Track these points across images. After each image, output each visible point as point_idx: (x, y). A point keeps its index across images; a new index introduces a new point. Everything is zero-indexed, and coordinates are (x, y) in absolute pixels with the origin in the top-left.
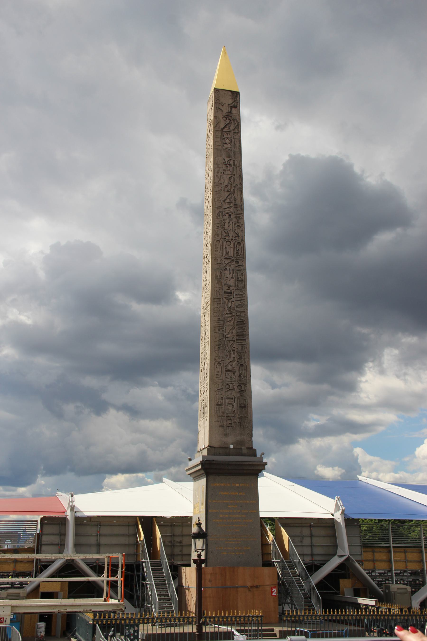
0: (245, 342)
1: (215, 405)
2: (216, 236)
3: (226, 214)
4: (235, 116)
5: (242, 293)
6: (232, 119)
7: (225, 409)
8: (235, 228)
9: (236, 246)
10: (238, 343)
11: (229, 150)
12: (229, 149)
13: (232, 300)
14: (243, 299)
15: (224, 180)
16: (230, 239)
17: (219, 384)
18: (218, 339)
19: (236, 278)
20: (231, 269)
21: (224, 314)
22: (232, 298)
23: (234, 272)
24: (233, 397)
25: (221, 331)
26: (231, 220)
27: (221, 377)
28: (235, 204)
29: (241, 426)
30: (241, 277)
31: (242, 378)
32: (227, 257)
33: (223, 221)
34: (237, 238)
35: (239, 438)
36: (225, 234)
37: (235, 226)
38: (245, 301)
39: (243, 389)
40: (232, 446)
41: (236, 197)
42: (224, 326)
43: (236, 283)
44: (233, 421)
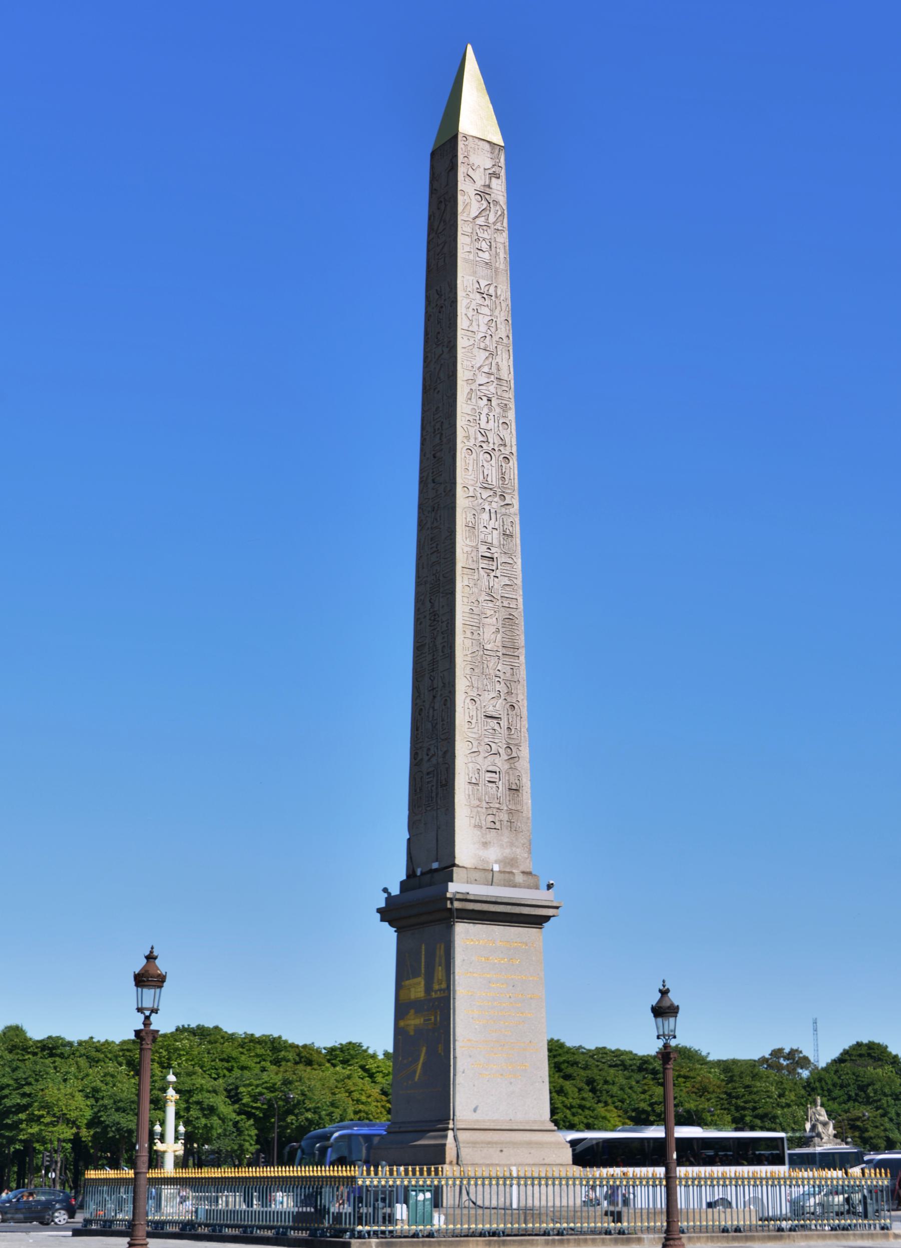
0: (517, 661)
1: (467, 783)
2: (465, 441)
3: (482, 397)
4: (497, 194)
5: (511, 562)
6: (490, 201)
7: (484, 793)
8: (498, 426)
9: (500, 464)
10: (505, 663)
11: (487, 263)
12: (487, 261)
13: (493, 574)
14: (513, 573)
15: (479, 326)
16: (490, 449)
17: (473, 742)
18: (470, 652)
19: (501, 531)
20: (493, 511)
21: (480, 601)
22: (493, 570)
23: (498, 516)
24: (498, 770)
25: (476, 636)
26: (492, 409)
27: (476, 728)
28: (498, 377)
29: (511, 827)
30: (511, 529)
31: (513, 732)
32: (484, 485)
33: (478, 411)
34: (502, 448)
35: (507, 851)
36: (481, 438)
37: (498, 422)
38: (516, 578)
39: (514, 755)
40: (496, 868)
41: (499, 364)
42: (481, 624)
43: (502, 540)
44: (497, 818)
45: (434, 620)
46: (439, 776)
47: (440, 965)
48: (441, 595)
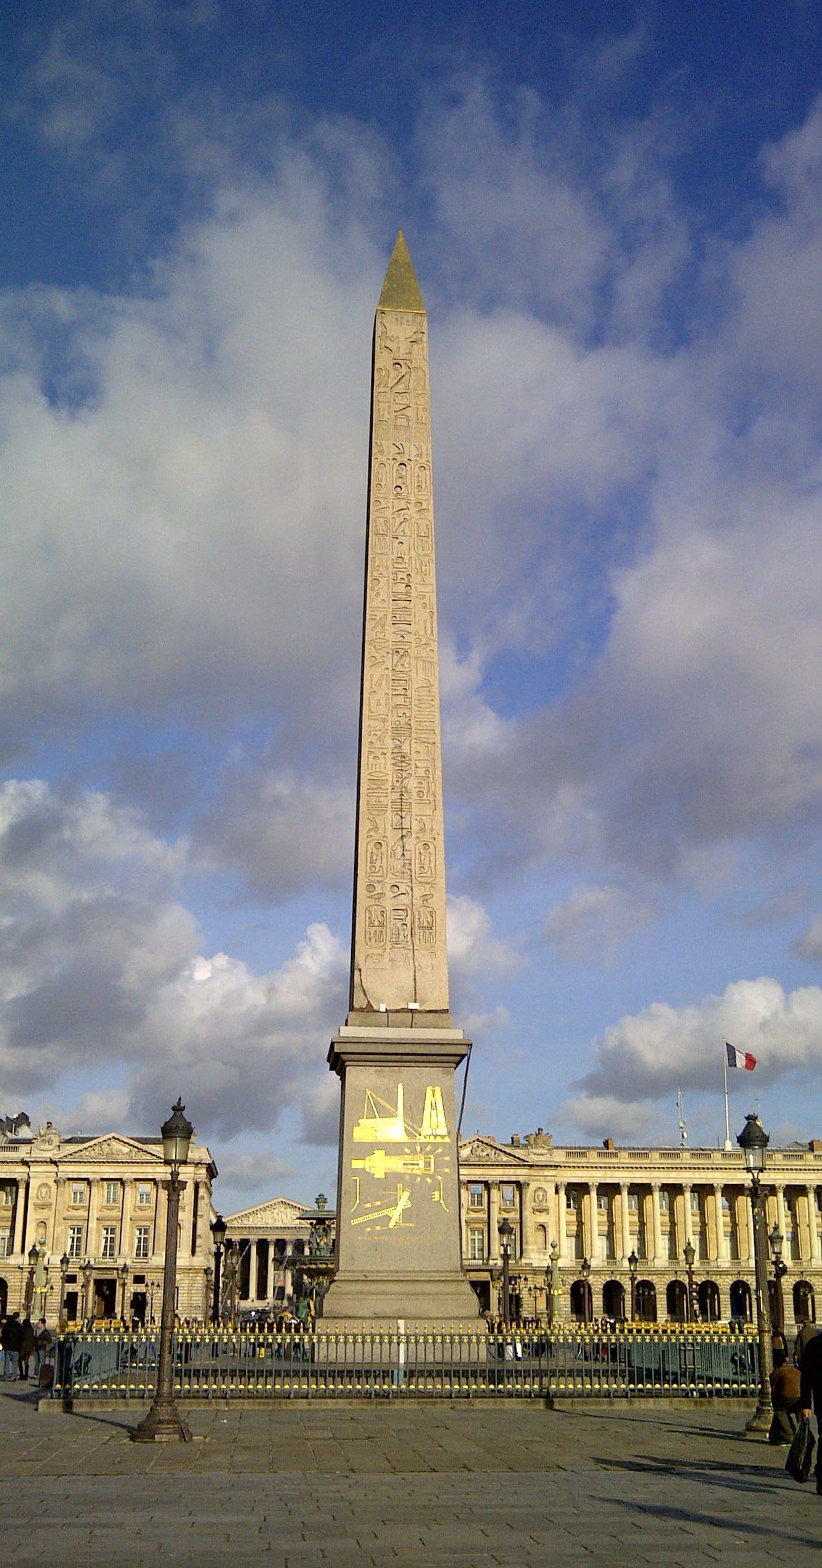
45: (402, 762)
46: (417, 917)
48: (414, 741)
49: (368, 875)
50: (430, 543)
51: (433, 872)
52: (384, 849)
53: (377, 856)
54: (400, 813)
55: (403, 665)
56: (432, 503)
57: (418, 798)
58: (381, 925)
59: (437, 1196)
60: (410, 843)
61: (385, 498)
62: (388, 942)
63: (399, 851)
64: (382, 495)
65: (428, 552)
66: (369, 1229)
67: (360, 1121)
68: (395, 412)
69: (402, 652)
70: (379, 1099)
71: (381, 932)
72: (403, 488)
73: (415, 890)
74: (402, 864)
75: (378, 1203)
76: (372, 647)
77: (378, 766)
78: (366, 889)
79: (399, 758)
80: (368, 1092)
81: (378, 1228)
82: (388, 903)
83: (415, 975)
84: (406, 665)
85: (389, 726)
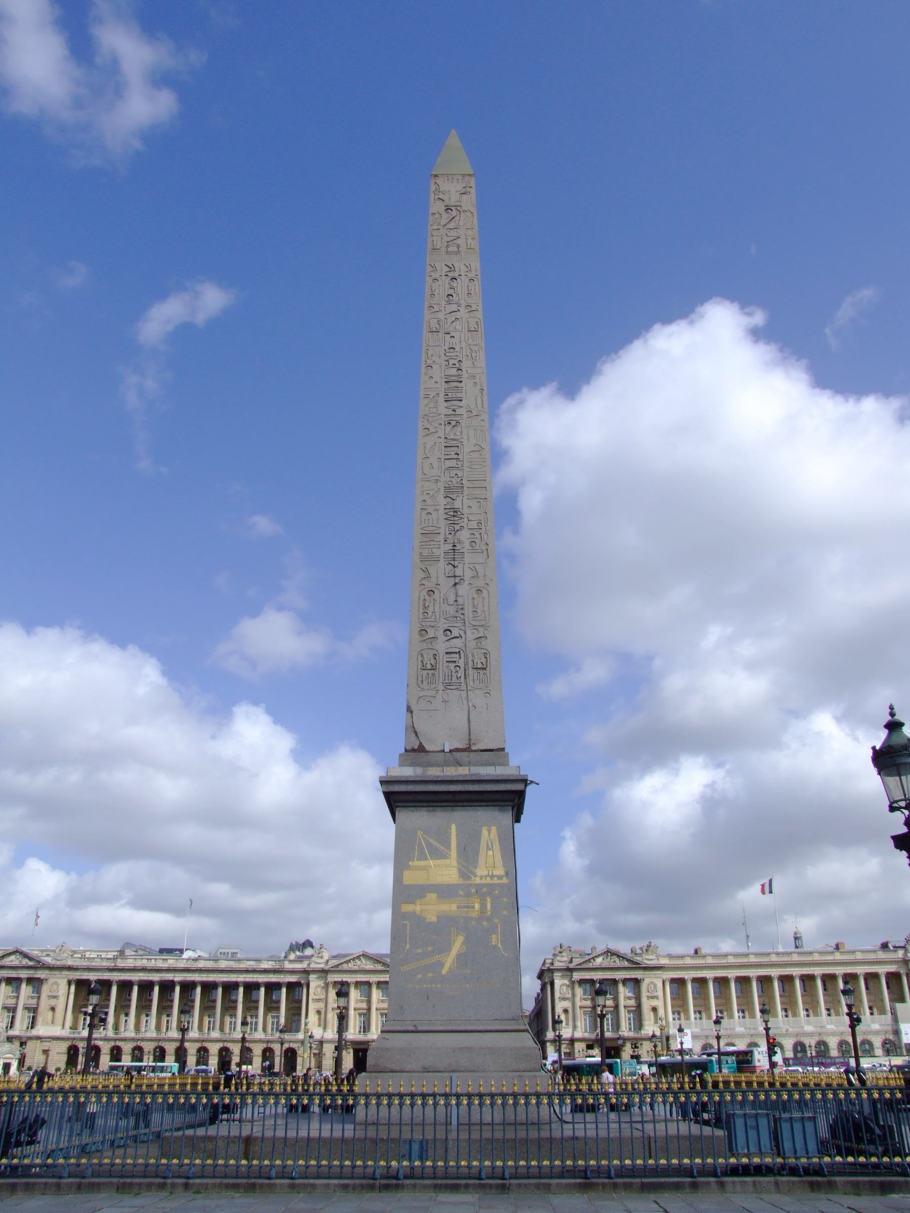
46: (470, 659)
47: (488, 849)
49: (420, 620)
50: (480, 336)
51: (487, 615)
52: (436, 596)
53: (430, 602)
54: (452, 562)
55: (455, 434)
56: (481, 305)
57: (471, 548)
58: (433, 668)
59: (495, 939)
60: (463, 589)
61: (438, 304)
62: (441, 685)
63: (452, 598)
64: (434, 302)
65: (477, 342)
66: (420, 976)
67: (411, 863)
68: (447, 242)
69: (453, 423)
70: (431, 841)
71: (433, 675)
72: (454, 297)
73: (469, 632)
74: (455, 609)
75: (430, 948)
76: (426, 421)
77: (431, 521)
78: (419, 634)
79: (452, 513)
80: (419, 833)
81: (430, 975)
82: (442, 645)
83: (469, 716)
84: (458, 433)
85: (441, 485)
